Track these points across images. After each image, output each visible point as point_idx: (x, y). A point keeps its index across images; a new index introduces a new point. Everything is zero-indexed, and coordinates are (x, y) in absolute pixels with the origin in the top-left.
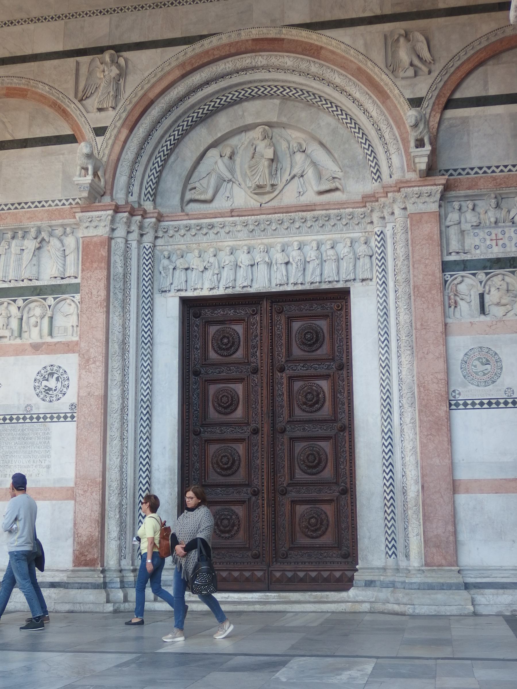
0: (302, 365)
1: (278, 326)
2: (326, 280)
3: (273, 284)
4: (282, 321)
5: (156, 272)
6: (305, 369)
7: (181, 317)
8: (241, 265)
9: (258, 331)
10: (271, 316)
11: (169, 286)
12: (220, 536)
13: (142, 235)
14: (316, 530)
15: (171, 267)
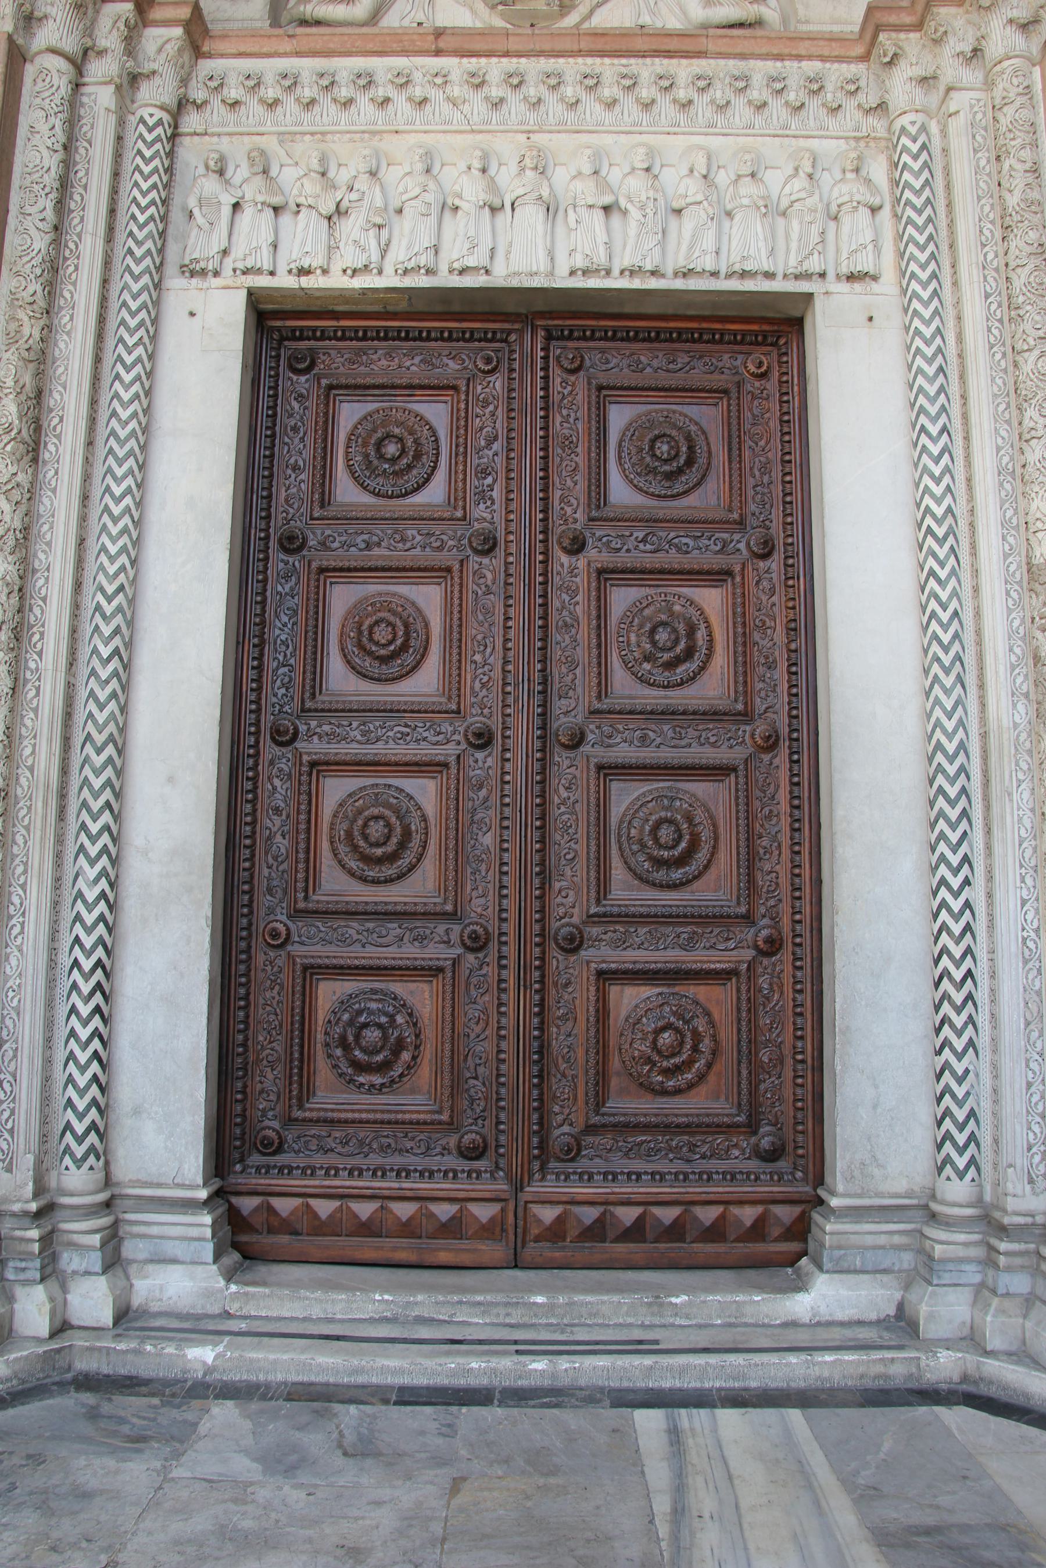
0: (641, 535)
1: (565, 412)
2: (737, 268)
3: (563, 267)
4: (580, 397)
5: (176, 216)
6: (648, 547)
7: (251, 362)
8: (457, 202)
9: (498, 425)
10: (546, 378)
11: (218, 258)
12: (351, 1081)
13: (134, 79)
14: (678, 1069)
15: (228, 200)
